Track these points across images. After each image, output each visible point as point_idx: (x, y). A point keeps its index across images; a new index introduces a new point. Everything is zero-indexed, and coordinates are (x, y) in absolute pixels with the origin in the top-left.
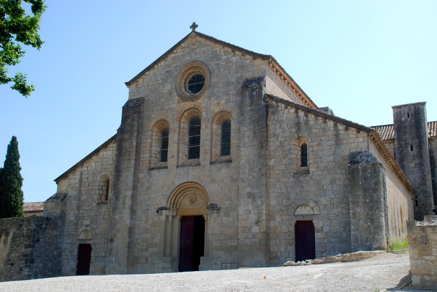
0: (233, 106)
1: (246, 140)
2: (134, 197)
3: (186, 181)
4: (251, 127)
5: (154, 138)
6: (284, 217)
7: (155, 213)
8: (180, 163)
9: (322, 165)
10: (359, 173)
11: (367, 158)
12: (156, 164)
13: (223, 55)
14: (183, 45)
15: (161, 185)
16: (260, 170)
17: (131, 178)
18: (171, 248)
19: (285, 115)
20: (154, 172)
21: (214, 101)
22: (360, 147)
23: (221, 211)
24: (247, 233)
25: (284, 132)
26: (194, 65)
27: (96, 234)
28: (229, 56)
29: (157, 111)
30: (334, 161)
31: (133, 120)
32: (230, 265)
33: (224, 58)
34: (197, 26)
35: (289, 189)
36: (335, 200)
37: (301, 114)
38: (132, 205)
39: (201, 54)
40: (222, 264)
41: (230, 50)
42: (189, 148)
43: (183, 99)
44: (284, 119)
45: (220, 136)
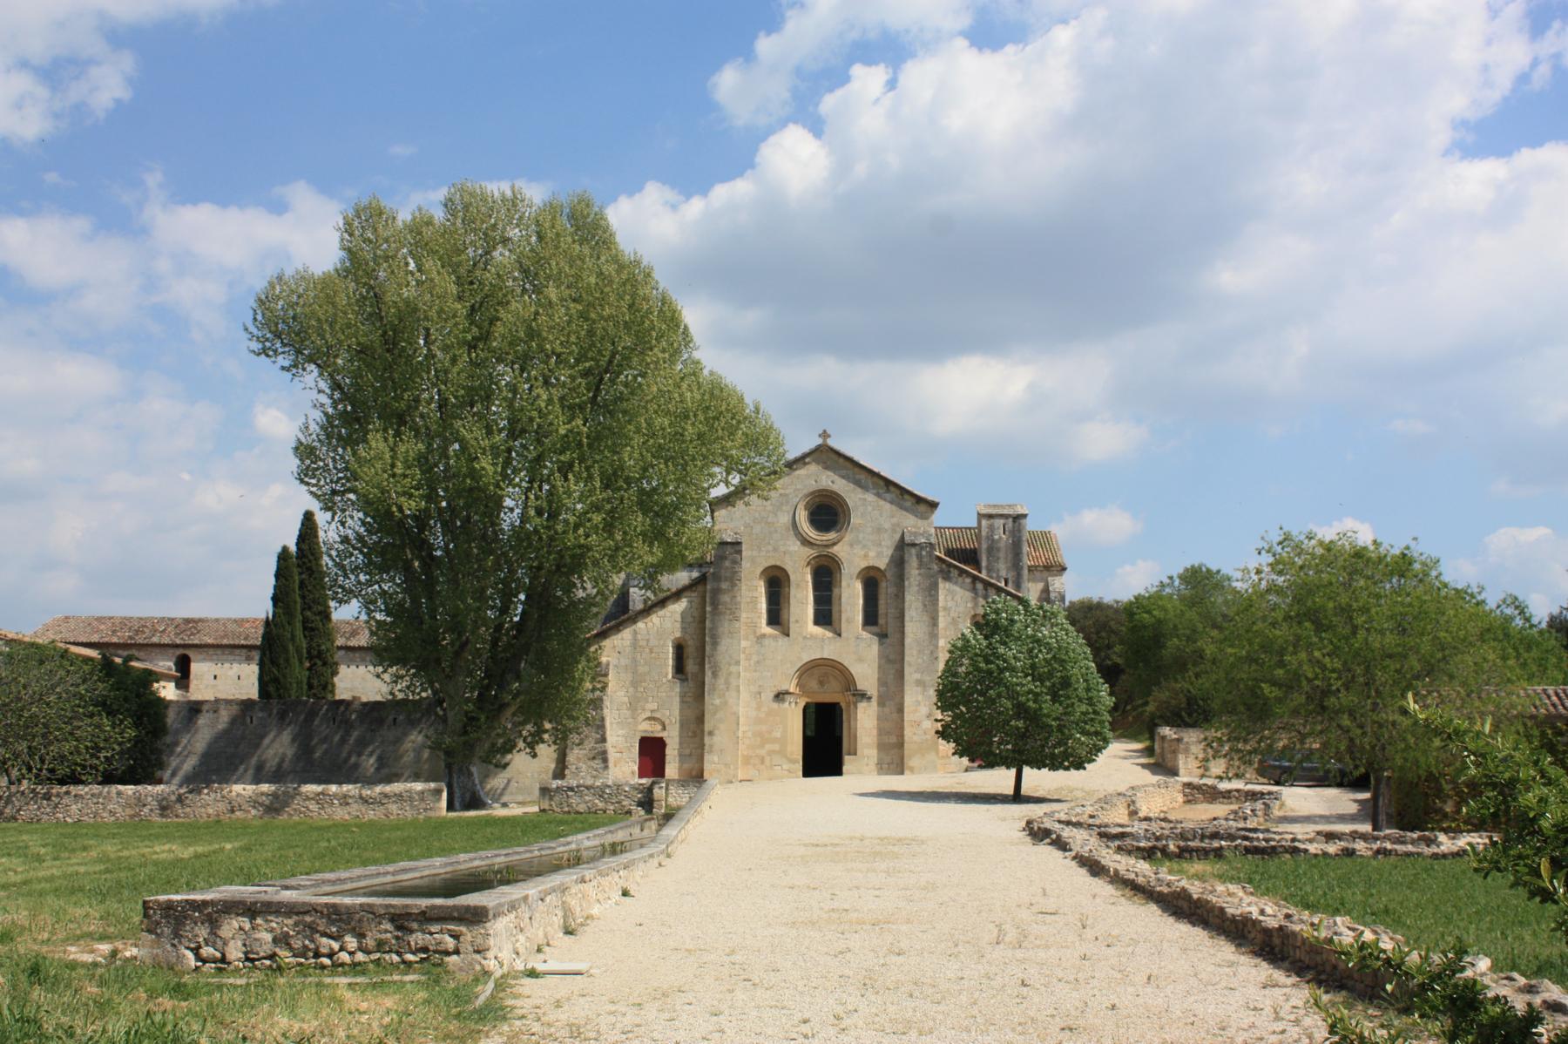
21: (858, 551)
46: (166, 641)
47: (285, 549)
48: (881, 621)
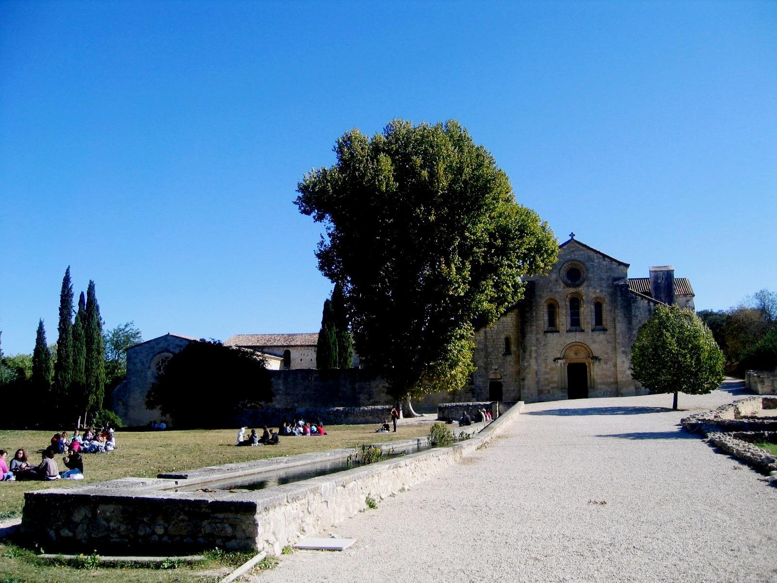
1: (619, 318)
7: (552, 362)
8: (568, 329)
14: (564, 247)
19: (641, 304)
20: (549, 334)
21: (591, 289)
23: (602, 361)
28: (601, 260)
29: (547, 292)
33: (597, 261)
34: (574, 235)
37: (652, 304)
39: (578, 255)
41: (601, 256)
43: (567, 285)
46: (279, 344)
47: (327, 300)
48: (604, 323)
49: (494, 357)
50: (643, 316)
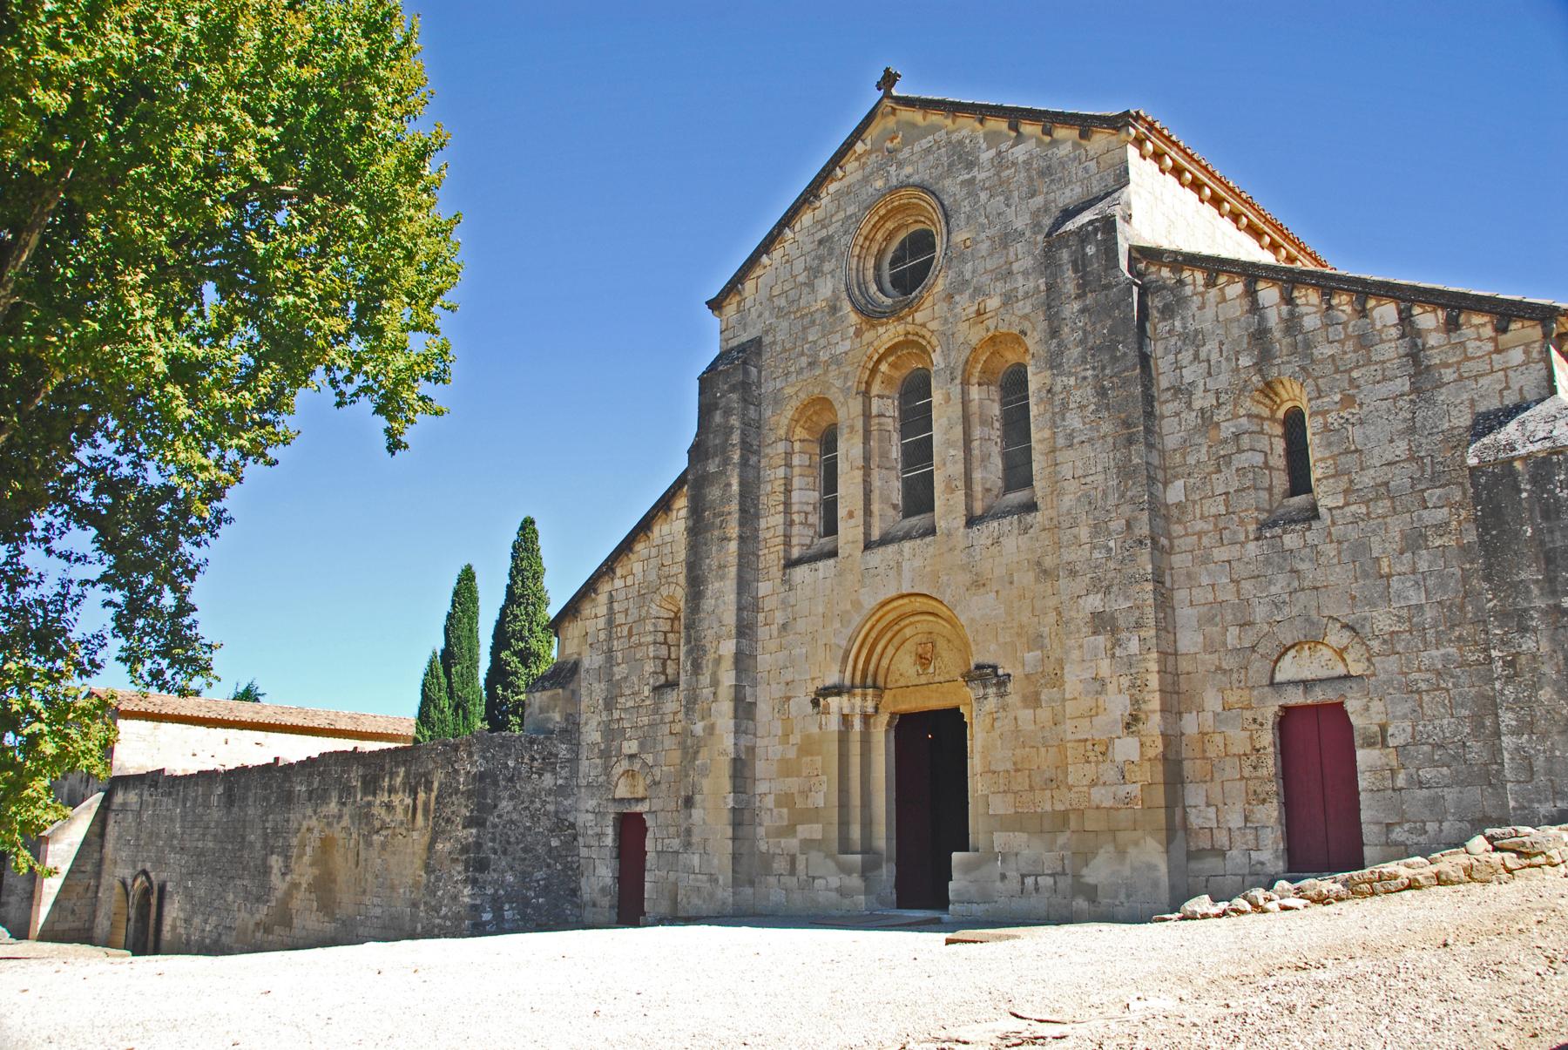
0: (1028, 310)
2: (743, 661)
3: (894, 594)
4: (1090, 373)
5: (796, 460)
6: (1232, 698)
8: (876, 535)
9: (1366, 479)
10: (1520, 491)
11: (1548, 427)
12: (809, 547)
13: (984, 146)
14: (859, 147)
15: (818, 616)
16: (1129, 525)
17: (731, 597)
18: (867, 824)
19: (1210, 312)
20: (800, 573)
21: (965, 305)
22: (1516, 387)
23: (1010, 687)
24: (1097, 763)
25: (1210, 374)
26: (895, 202)
27: (656, 783)
29: (800, 371)
30: (1411, 459)
31: (728, 412)
32: (1050, 881)
33: (986, 156)
35: (1247, 586)
36: (1429, 614)
37: (1269, 294)
38: (738, 689)
40: (1023, 876)
41: (1002, 125)
42: (906, 482)
44: (1207, 326)
45: (997, 425)
49: (630, 704)
50: (1223, 380)
